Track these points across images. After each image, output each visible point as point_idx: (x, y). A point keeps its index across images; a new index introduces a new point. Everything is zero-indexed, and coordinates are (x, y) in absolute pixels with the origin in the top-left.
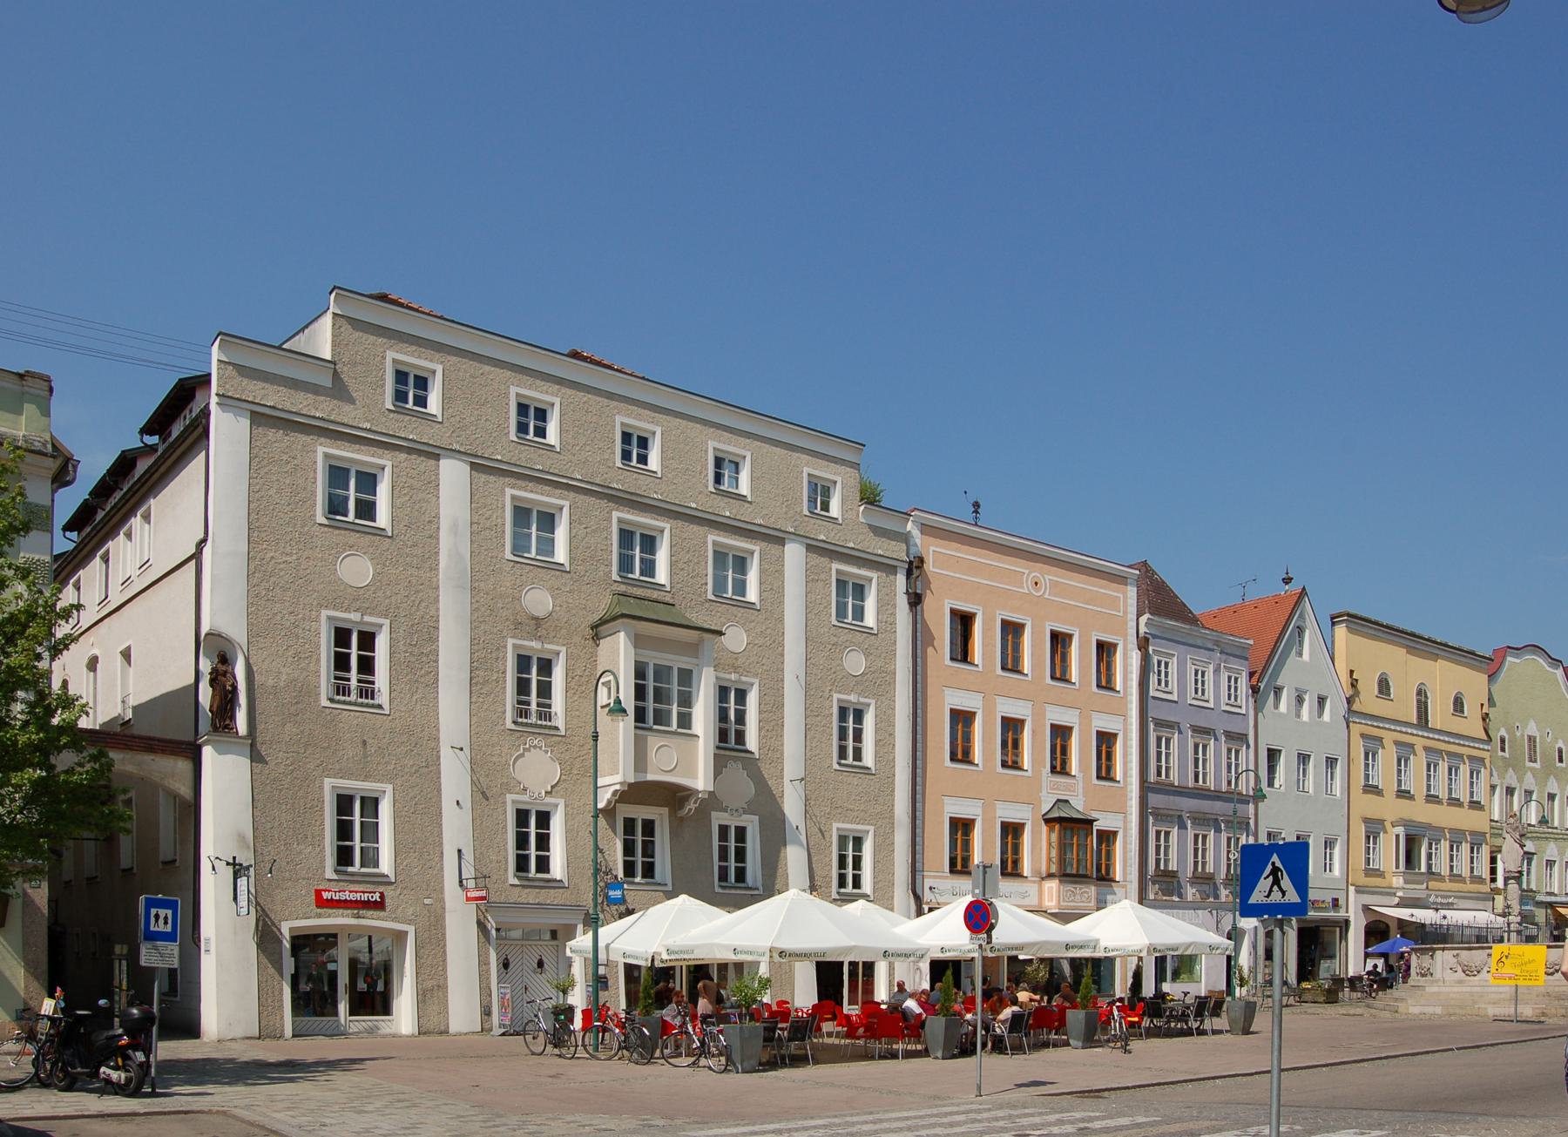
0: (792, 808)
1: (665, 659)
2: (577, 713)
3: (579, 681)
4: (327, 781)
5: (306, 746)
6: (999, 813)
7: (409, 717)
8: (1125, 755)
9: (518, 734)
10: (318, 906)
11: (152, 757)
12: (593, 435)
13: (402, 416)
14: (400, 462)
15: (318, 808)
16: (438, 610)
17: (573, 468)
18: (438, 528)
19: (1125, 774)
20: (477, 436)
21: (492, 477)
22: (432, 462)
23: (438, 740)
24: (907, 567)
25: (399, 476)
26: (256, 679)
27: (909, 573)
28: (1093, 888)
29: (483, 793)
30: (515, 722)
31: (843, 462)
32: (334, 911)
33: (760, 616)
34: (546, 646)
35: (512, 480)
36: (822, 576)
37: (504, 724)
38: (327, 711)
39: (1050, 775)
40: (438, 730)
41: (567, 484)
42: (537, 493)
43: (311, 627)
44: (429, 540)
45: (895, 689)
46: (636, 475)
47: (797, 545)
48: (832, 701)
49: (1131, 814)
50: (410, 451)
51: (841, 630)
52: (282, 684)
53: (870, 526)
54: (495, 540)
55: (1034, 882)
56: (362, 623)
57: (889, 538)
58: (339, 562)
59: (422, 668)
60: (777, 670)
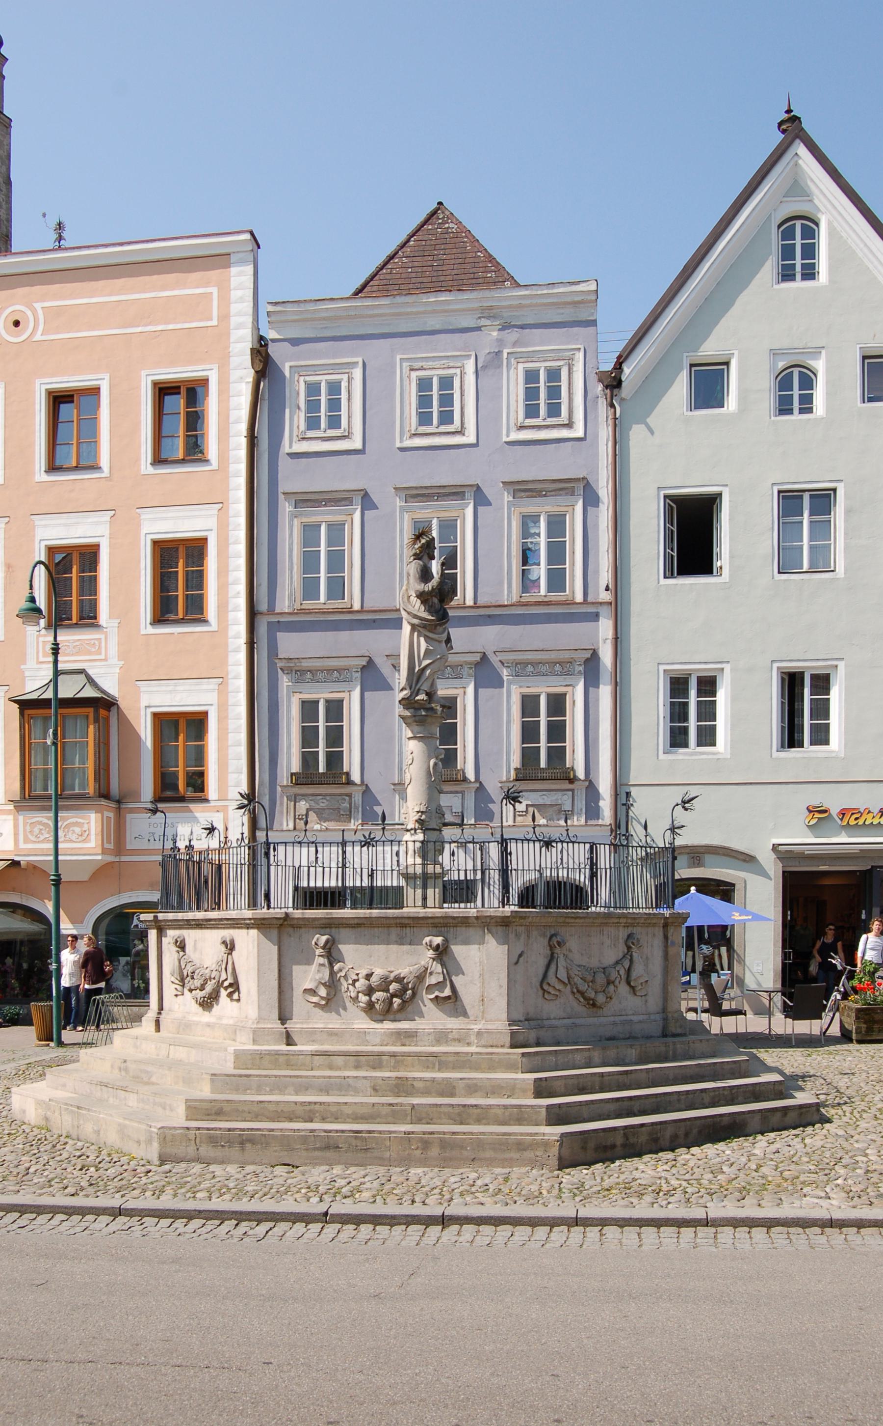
19: (223, 607)
55: (8, 812)
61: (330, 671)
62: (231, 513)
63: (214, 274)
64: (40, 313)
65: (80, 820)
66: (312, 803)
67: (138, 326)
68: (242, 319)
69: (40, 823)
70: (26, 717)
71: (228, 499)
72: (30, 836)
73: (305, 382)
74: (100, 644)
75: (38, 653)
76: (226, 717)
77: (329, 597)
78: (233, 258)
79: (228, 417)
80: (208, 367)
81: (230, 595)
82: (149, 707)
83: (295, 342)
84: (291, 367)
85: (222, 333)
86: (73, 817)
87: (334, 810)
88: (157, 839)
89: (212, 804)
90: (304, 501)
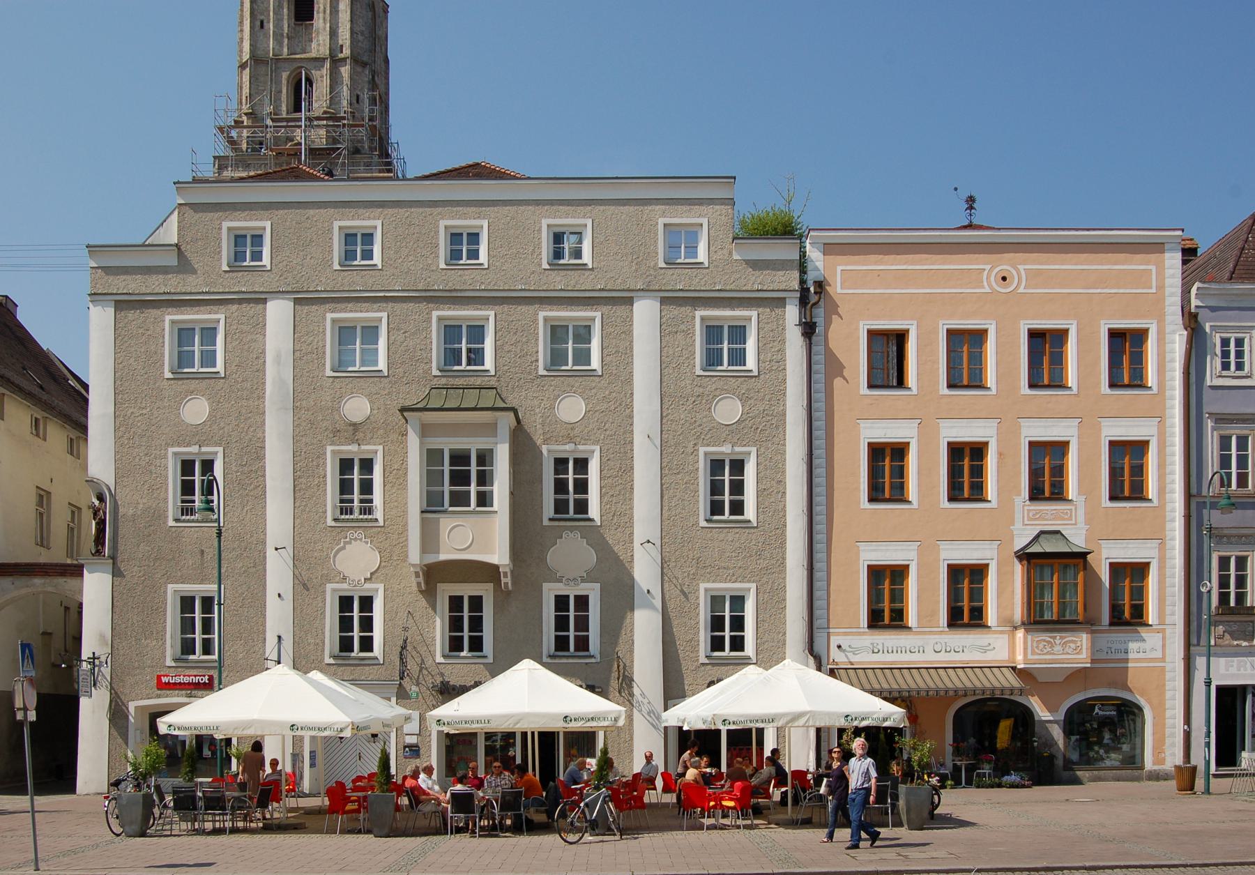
0: (645, 571)
1: (460, 443)
2: (396, 504)
3: (396, 475)
4: (170, 586)
5: (156, 559)
6: (943, 555)
7: (240, 526)
8: (1162, 466)
9: (339, 530)
10: (158, 689)
11: (65, 580)
12: (415, 245)
13: (236, 274)
14: (232, 313)
15: (162, 609)
16: (264, 432)
17: (395, 281)
18: (265, 362)
19: (1162, 490)
20: (303, 274)
21: (314, 307)
22: (261, 306)
23: (265, 543)
24: (799, 296)
25: (231, 325)
26: (120, 510)
27: (804, 301)
28: (1084, 636)
29: (304, 585)
30: (336, 520)
31: (711, 201)
32: (171, 692)
33: (603, 382)
34: (363, 447)
35: (333, 305)
36: (683, 327)
37: (326, 522)
38: (173, 529)
39: (1028, 503)
40: (266, 534)
41: (385, 296)
42: (356, 311)
43: (161, 463)
44: (257, 373)
45: (785, 432)
46: (460, 272)
47: (648, 301)
48: (697, 455)
49: (1173, 539)
50: (240, 301)
51: (708, 379)
52: (139, 513)
53: (747, 262)
54: (316, 361)
56: (199, 453)
57: (773, 269)
58: (182, 407)
59: (251, 484)
60: (625, 433)
61: (1240, 536)
62: (1167, 425)
63: (1153, 257)
64: (1023, 273)
65: (1074, 639)
66: (1227, 627)
67: (1097, 288)
68: (1173, 290)
69: (1044, 641)
70: (1032, 564)
71: (1165, 415)
72: (1036, 650)
73: (1220, 337)
74: (1071, 512)
75: (1023, 517)
76: (1165, 567)
77: (1239, 486)
78: (1167, 246)
79: (1165, 358)
80: (1150, 321)
81: (1167, 482)
82: (1108, 558)
83: (1213, 309)
84: (1211, 326)
85: (1159, 299)
86: (1069, 637)
87: (1242, 632)
88: (1113, 651)
89: (1154, 627)
90: (1220, 419)
